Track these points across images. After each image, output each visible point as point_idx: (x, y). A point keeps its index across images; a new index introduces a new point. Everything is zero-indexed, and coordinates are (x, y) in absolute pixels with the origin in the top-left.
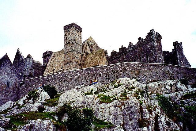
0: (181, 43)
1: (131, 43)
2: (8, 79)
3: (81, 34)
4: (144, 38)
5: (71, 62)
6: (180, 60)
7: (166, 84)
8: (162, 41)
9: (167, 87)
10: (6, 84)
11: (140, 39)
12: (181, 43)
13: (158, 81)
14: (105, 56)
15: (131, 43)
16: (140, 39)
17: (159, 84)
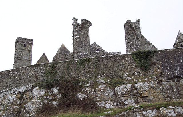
12: (138, 21)
17: (4, 94)
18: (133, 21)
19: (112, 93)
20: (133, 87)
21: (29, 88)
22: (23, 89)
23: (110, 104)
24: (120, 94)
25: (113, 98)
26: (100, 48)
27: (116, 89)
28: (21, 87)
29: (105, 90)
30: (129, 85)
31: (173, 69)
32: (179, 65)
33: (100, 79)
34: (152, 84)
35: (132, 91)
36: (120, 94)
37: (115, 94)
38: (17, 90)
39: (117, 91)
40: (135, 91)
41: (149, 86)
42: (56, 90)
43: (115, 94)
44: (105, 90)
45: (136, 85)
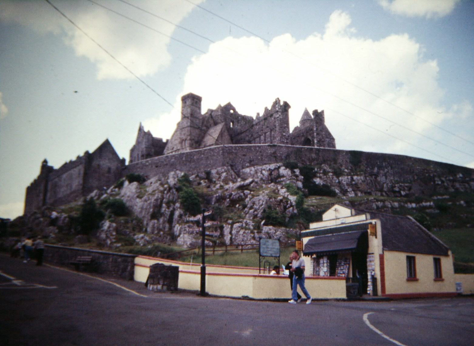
0: (323, 112)
1: (258, 114)
2: (109, 165)
3: (200, 105)
4: (270, 108)
5: (186, 140)
6: (318, 134)
7: (264, 170)
8: (290, 111)
9: (264, 172)
10: (106, 170)
11: (266, 109)
12: (323, 112)
13: (256, 166)
14: (226, 131)
15: (258, 114)
16: (266, 109)
18: (319, 111)
19: (337, 181)
20: (352, 179)
21: (277, 167)
22: (272, 166)
23: (338, 190)
24: (345, 183)
25: (338, 184)
26: (234, 109)
27: (340, 178)
28: (270, 165)
29: (333, 178)
30: (349, 177)
31: (373, 168)
32: (377, 167)
33: (326, 167)
34: (362, 177)
35: (351, 182)
36: (345, 183)
37: (339, 182)
38: (268, 167)
39: (342, 180)
40: (353, 182)
41: (361, 179)
42: (297, 171)
43: (339, 182)
44: (333, 178)
45: (355, 177)
